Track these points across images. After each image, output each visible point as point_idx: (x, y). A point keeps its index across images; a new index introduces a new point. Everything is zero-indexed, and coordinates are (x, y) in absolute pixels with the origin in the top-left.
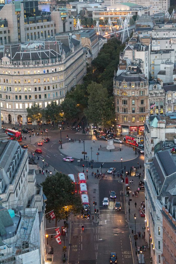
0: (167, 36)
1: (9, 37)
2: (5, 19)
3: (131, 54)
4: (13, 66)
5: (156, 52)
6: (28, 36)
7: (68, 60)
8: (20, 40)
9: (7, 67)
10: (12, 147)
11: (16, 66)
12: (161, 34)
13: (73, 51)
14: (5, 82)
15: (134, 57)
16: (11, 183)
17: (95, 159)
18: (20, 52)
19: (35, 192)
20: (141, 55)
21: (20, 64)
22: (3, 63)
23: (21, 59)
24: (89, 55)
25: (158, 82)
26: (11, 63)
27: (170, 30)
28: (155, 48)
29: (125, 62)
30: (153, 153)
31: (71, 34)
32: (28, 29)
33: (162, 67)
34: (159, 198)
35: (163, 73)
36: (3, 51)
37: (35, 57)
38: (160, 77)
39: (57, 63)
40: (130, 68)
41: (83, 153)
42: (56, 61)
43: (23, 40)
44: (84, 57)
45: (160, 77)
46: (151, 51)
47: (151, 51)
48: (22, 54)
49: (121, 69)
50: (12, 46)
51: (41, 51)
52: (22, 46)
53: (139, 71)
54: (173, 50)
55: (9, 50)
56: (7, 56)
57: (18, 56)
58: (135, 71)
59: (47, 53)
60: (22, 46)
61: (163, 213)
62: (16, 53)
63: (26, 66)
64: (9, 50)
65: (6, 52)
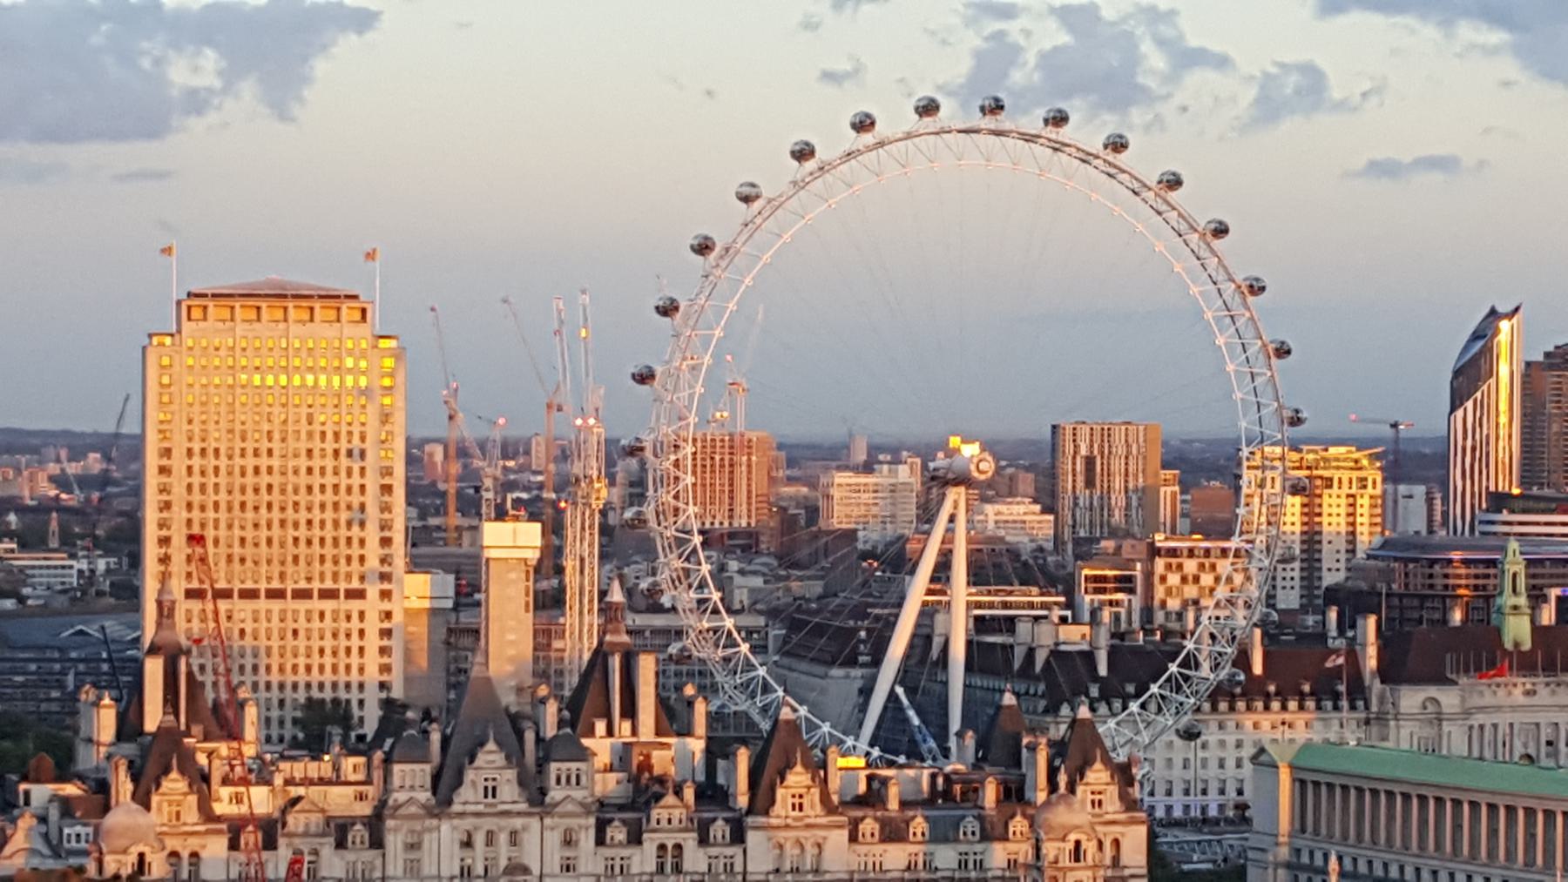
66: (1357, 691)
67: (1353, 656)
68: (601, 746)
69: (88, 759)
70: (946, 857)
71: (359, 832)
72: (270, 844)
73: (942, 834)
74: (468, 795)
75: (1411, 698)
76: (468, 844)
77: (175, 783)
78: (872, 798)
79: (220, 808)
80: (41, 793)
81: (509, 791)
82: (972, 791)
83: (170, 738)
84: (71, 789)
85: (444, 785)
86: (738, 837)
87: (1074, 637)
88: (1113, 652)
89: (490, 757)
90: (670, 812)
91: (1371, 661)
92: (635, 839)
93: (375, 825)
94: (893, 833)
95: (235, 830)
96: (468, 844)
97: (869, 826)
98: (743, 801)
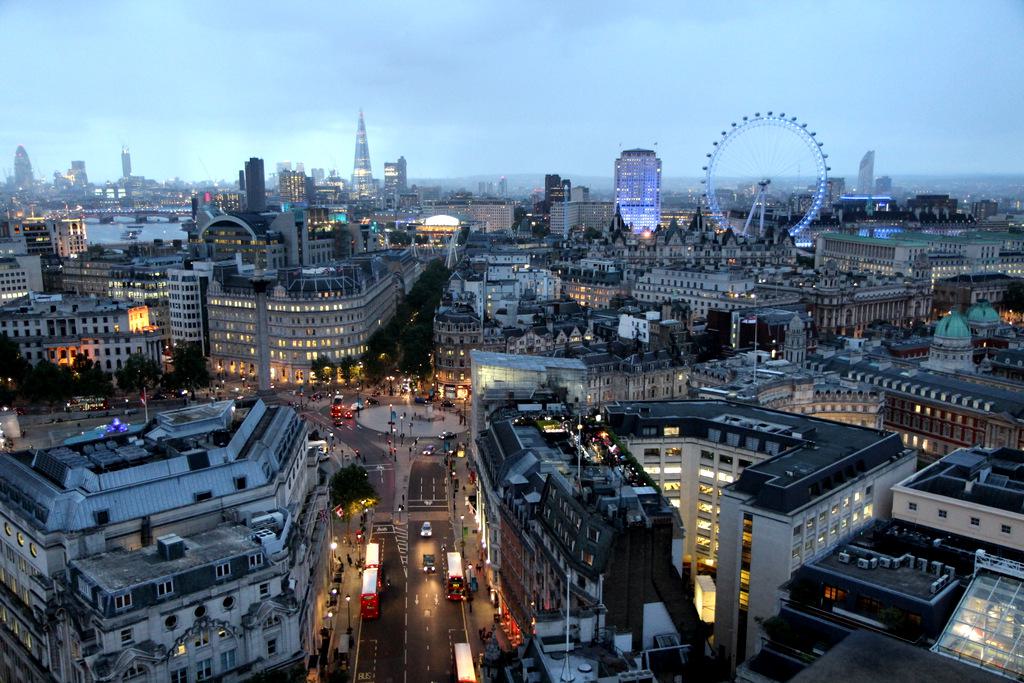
0: (510, 262)
1: (286, 258)
2: (280, 233)
3: (459, 285)
4: (290, 299)
5: (495, 283)
6: (314, 258)
7: (371, 291)
8: (301, 260)
10: (285, 415)
11: (295, 300)
12: (501, 259)
13: (377, 278)
15: (463, 289)
16: (281, 469)
17: (406, 432)
19: (317, 481)
20: (473, 287)
24: (400, 286)
25: (497, 324)
27: (512, 254)
28: (494, 278)
29: (450, 296)
30: (487, 424)
31: (374, 255)
32: (313, 247)
33: (502, 304)
34: (495, 489)
35: (502, 312)
37: (323, 289)
38: (500, 317)
39: (355, 296)
40: (457, 304)
41: (389, 423)
42: (352, 294)
43: (305, 263)
44: (393, 288)
45: (500, 317)
46: (488, 281)
47: (488, 281)
49: (444, 305)
51: (330, 278)
52: (304, 271)
53: (469, 309)
54: (518, 281)
57: (298, 283)
58: (465, 309)
59: (340, 281)
60: (304, 271)
61: (500, 509)
66: (838, 223)
67: (838, 217)
68: (697, 233)
69: (604, 235)
70: (758, 254)
71: (651, 249)
72: (636, 250)
73: (759, 249)
74: (671, 242)
75: (848, 225)
76: (671, 250)
77: (619, 239)
78: (745, 243)
79: (628, 243)
80: (596, 241)
81: (679, 241)
82: (763, 242)
83: (618, 231)
84: (602, 240)
85: (667, 239)
86: (720, 250)
87: (784, 214)
88: (792, 217)
89: (676, 235)
90: (707, 246)
91: (841, 218)
92: (701, 250)
93: (655, 247)
94: (749, 249)
95: (630, 248)
96: (671, 250)
97: (744, 248)
98: (720, 242)
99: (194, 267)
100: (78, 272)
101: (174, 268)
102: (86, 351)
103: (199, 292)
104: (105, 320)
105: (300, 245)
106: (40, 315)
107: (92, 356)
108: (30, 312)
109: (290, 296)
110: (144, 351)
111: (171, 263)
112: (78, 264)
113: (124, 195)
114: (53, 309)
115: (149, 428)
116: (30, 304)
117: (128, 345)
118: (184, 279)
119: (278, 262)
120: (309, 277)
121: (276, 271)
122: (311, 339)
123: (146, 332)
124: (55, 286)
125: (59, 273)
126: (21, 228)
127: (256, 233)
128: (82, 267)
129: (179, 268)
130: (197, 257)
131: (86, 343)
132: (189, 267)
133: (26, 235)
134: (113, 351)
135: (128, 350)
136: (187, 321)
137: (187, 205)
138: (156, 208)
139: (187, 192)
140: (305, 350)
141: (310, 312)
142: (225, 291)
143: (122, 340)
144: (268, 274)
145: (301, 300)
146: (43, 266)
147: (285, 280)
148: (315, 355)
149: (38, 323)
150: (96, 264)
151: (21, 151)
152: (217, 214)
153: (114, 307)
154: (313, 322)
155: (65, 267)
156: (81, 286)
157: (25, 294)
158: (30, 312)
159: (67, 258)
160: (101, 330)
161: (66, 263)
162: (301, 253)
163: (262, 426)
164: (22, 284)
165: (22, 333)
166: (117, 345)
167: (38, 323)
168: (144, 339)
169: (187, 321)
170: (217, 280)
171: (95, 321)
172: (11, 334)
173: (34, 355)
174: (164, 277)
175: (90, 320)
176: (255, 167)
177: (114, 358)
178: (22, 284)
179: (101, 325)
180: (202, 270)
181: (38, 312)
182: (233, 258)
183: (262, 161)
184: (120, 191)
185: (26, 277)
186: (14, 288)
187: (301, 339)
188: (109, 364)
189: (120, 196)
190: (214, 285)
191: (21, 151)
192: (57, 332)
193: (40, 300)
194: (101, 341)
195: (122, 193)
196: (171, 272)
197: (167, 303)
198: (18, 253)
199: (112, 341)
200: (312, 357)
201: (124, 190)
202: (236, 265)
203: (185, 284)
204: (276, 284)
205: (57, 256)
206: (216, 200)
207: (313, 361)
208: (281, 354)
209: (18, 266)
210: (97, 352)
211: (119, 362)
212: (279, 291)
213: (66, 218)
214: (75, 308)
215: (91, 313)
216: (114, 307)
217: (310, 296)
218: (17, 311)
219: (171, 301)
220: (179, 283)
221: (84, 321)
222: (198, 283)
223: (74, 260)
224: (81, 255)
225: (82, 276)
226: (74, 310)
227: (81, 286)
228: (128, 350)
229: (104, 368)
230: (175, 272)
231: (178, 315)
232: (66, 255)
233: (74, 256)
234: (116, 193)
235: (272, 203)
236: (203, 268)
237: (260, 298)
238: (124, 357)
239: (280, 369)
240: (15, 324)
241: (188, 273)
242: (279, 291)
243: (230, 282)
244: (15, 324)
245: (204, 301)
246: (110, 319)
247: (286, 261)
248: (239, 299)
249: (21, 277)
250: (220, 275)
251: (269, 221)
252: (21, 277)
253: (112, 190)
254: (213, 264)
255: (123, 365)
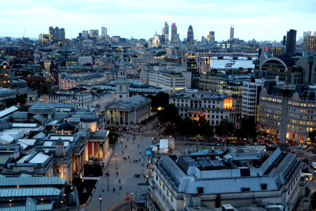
1: (302, 80)
2: (300, 67)
4: (301, 100)
9: (296, 100)
11: (304, 101)
14: (293, 110)
18: (308, 91)
21: (306, 99)
22: (293, 97)
23: (308, 95)
26: (299, 97)
36: (294, 89)
48: (309, 92)
50: (302, 86)
52: (311, 87)
55: (300, 88)
56: (298, 92)
60: (311, 87)
62: (305, 91)
63: (311, 101)
64: (300, 88)
65: (296, 89)
99: (256, 81)
100: (205, 80)
101: (246, 81)
102: (204, 115)
103: (256, 93)
104: (214, 103)
105: (310, 73)
106: (187, 98)
107: (206, 118)
108: (184, 96)
109: (301, 99)
110: (228, 118)
111: (246, 78)
112: (206, 77)
113: (229, 47)
114: (193, 95)
115: (225, 153)
116: (185, 93)
117: (222, 114)
118: (250, 86)
119: (297, 82)
120: (312, 89)
121: (295, 86)
122: (310, 121)
123: (231, 110)
124: (196, 86)
125: (198, 80)
126: (186, 60)
127: (288, 66)
128: (207, 78)
129: (248, 81)
130: (258, 76)
131: (205, 112)
132: (253, 81)
133: (187, 63)
134: (215, 117)
135: (222, 117)
136: (249, 106)
137: (256, 52)
138: (242, 53)
139: (257, 46)
140: (306, 126)
141: (311, 107)
142: (269, 94)
143: (220, 112)
144: (291, 87)
145: (307, 101)
146: (192, 77)
147: (300, 90)
148: (311, 129)
149: (187, 101)
150: (213, 77)
151: (191, 28)
152: (269, 57)
153: (218, 97)
154: (312, 112)
155: (201, 78)
156: (206, 86)
157: (184, 88)
158: (184, 96)
159: (202, 74)
160: (211, 107)
161: (201, 76)
162: (310, 78)
163: (278, 161)
164: (183, 84)
165: (180, 105)
166: (217, 114)
167: (187, 101)
168: (229, 113)
169: (249, 106)
170: (266, 88)
171: (209, 102)
172: (176, 105)
173: (184, 115)
174: (241, 84)
175: (207, 102)
176: (292, 34)
177: (215, 120)
178: (183, 84)
179: (212, 104)
180: (259, 83)
181: (187, 96)
182: (274, 78)
183: (296, 31)
184: (228, 45)
185: (185, 81)
186: (180, 86)
187: (305, 120)
188: (213, 122)
189: (227, 47)
190: (264, 90)
191: (191, 28)
192: (194, 106)
193: (189, 91)
194: (211, 112)
195: (228, 46)
196: (245, 83)
197: (241, 97)
198: (183, 71)
199: (215, 112)
200: (310, 130)
201: (229, 45)
202: (276, 82)
203: (250, 89)
204: (295, 92)
205: (198, 73)
206: (270, 50)
207: (310, 132)
208: (293, 127)
209: (182, 76)
210: (209, 116)
211: (217, 122)
212: (296, 95)
213: (204, 56)
214: (202, 96)
215: (209, 99)
216: (218, 97)
217: (311, 100)
218: (180, 95)
219: (243, 96)
220: (248, 88)
221: (205, 102)
222: (256, 89)
223: (205, 75)
224: (208, 73)
225: (207, 82)
226: (202, 97)
227: (206, 86)
228: (222, 117)
229: (211, 124)
230: (247, 83)
231: (246, 103)
232: (202, 72)
233: (205, 73)
234: (226, 46)
235: (298, 52)
236: (259, 82)
237: (285, 98)
238: (220, 120)
239: (292, 134)
240: (178, 101)
241: (252, 84)
242: (296, 95)
243: (272, 89)
244: (178, 101)
245: (258, 97)
246: (216, 102)
247: (302, 81)
248: (275, 98)
249: (183, 81)
250: (267, 86)
251: (295, 61)
252: (183, 81)
253: (224, 45)
254: (265, 80)
255: (219, 124)
